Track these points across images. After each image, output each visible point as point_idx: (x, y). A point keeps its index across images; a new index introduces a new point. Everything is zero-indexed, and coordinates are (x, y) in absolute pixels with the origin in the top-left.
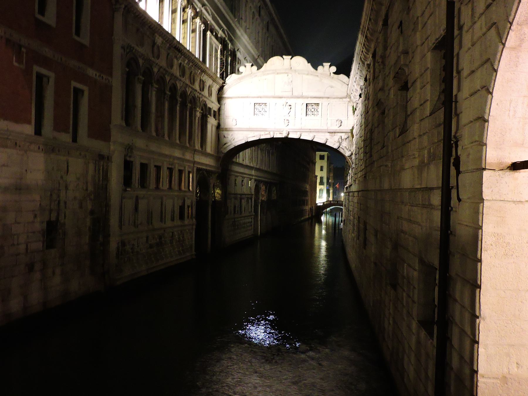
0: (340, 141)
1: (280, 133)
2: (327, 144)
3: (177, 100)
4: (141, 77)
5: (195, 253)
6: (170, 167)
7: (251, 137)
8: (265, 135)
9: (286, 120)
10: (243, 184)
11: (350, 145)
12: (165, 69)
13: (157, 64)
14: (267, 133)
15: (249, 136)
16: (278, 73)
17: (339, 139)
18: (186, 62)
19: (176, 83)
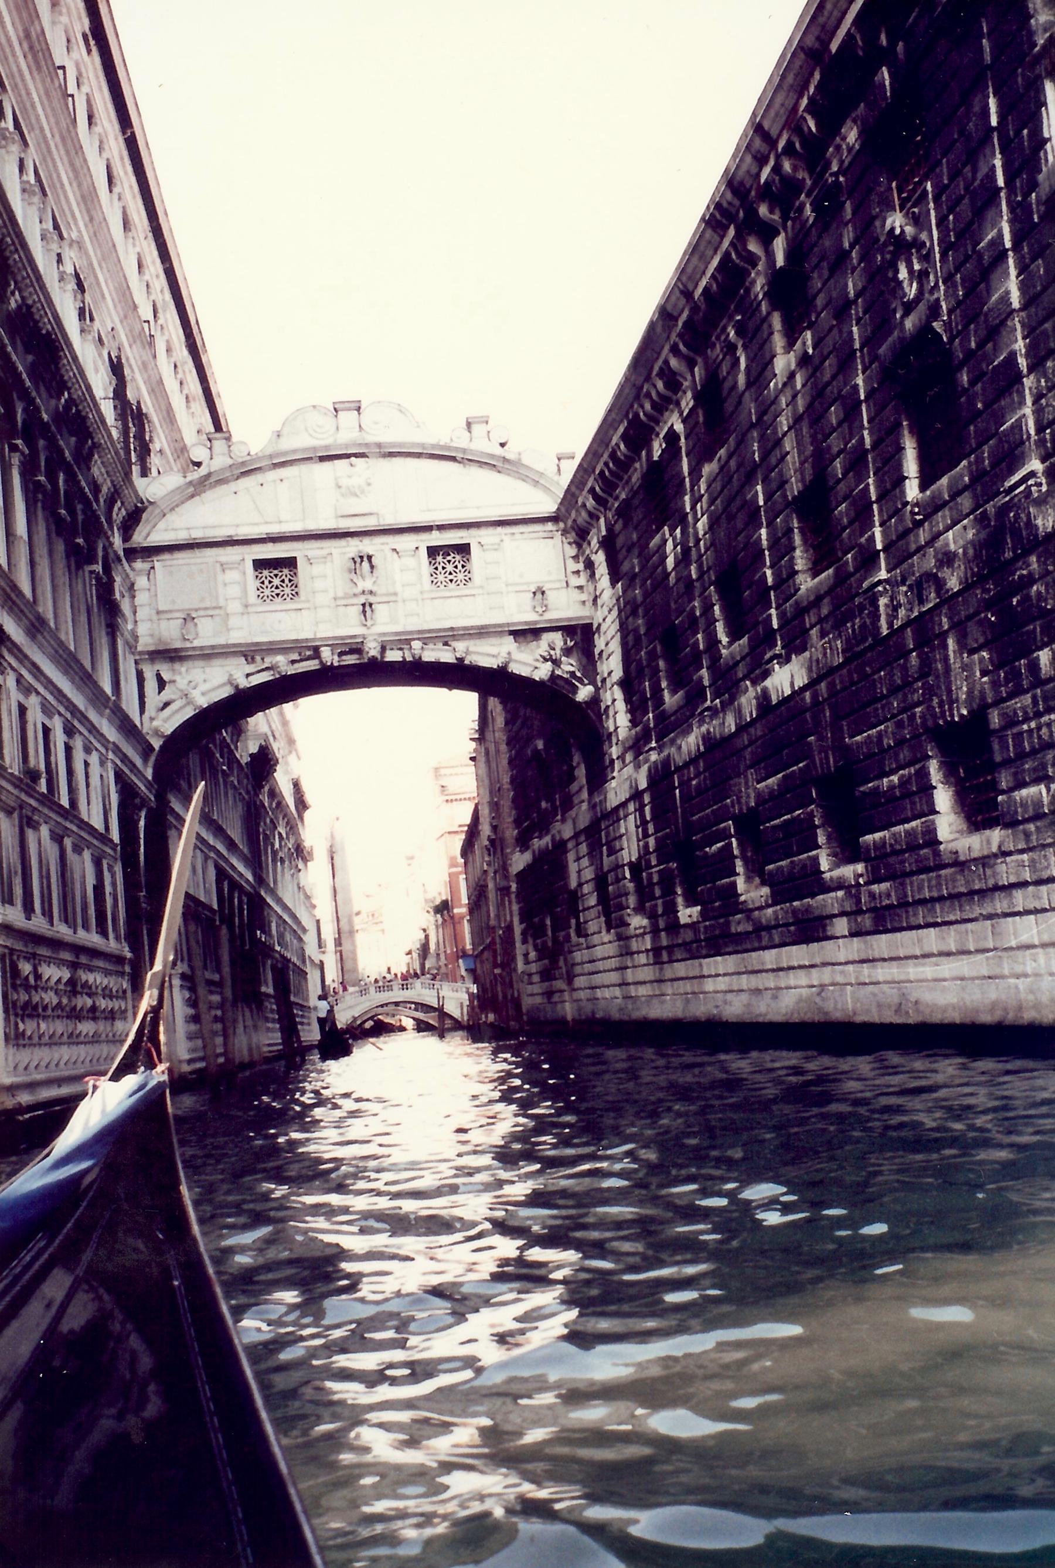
8: (301, 660)
15: (251, 668)
16: (322, 459)
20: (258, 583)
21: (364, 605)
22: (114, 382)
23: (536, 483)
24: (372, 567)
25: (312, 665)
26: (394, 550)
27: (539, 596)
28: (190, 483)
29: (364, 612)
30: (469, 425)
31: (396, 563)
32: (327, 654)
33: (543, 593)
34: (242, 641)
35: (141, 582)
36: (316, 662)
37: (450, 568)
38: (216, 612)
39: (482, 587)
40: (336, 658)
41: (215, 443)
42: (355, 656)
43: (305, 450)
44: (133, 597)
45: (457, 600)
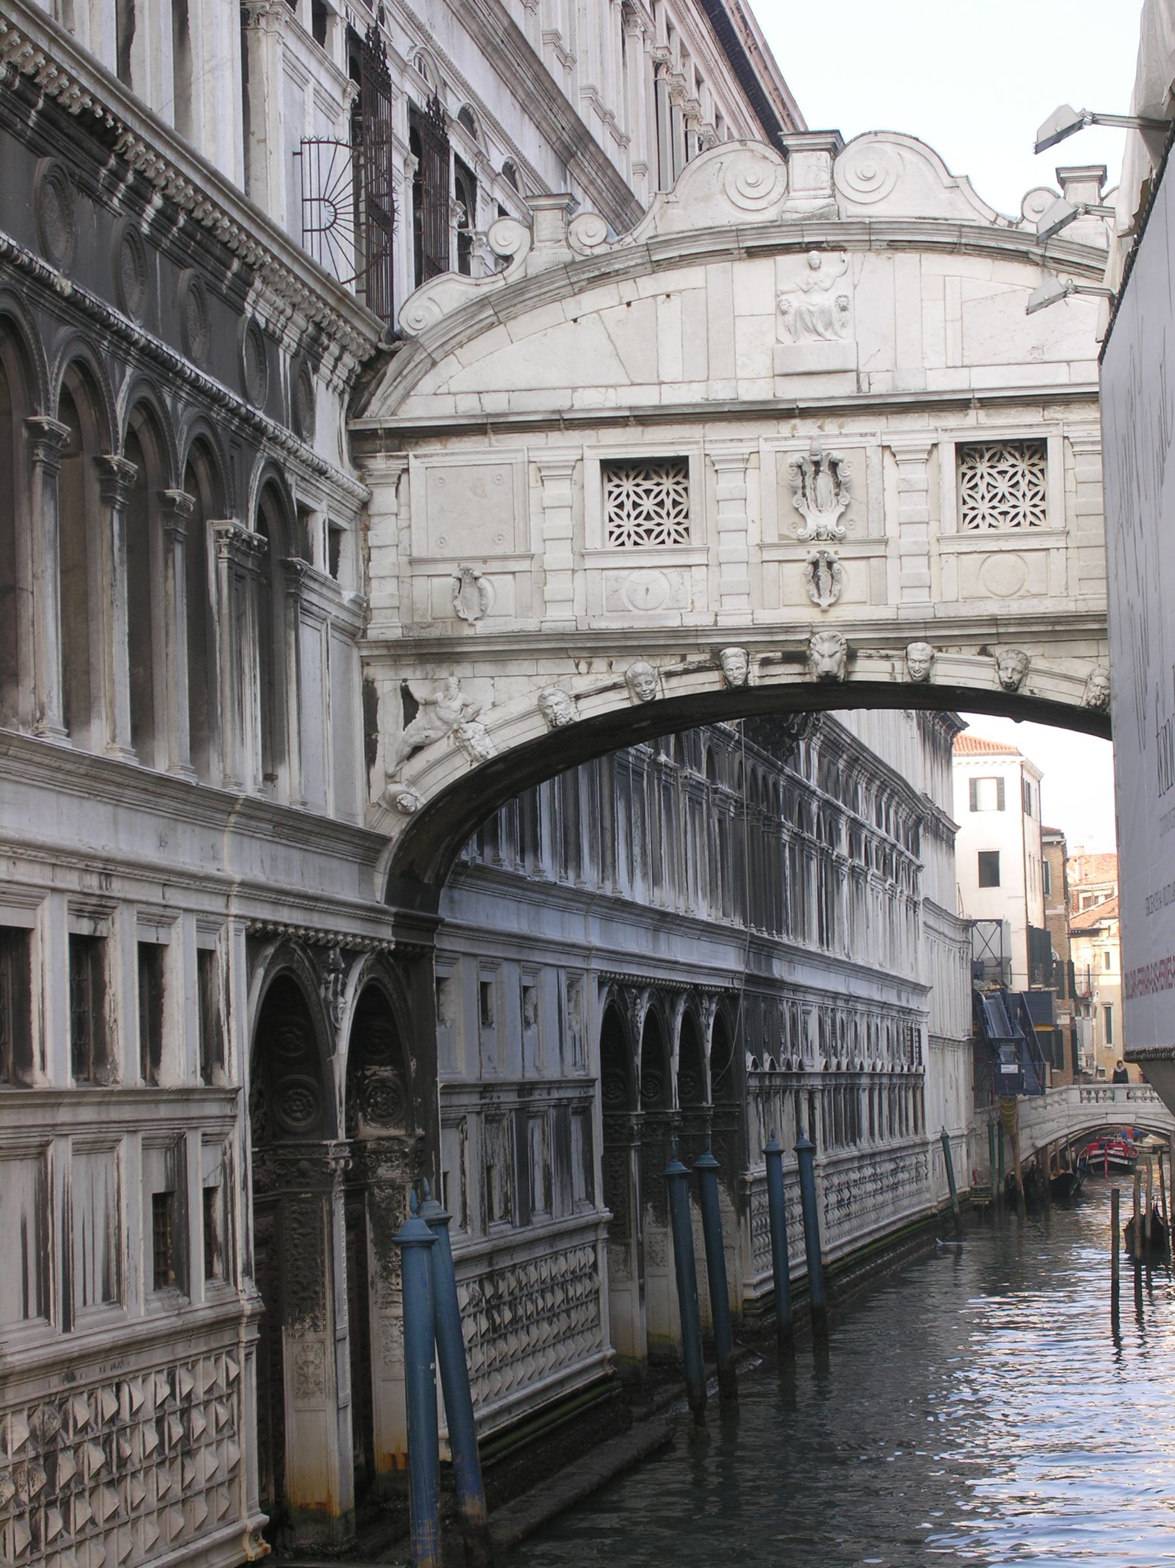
1: (790, 658)
5: (265, 1518)
6: (85, 928)
7: (587, 695)
8: (686, 672)
9: (822, 564)
10: (530, 1013)
12: (26, 270)
15: (582, 684)
16: (753, 253)
18: (150, 212)
20: (610, 507)
21: (815, 564)
22: (353, 90)
24: (838, 484)
25: (708, 682)
26: (884, 447)
28: (483, 302)
29: (816, 578)
30: (1062, 182)
32: (734, 659)
34: (569, 627)
35: (384, 498)
36: (715, 676)
37: (1003, 486)
38: (524, 565)
40: (755, 670)
42: (796, 668)
44: (367, 528)
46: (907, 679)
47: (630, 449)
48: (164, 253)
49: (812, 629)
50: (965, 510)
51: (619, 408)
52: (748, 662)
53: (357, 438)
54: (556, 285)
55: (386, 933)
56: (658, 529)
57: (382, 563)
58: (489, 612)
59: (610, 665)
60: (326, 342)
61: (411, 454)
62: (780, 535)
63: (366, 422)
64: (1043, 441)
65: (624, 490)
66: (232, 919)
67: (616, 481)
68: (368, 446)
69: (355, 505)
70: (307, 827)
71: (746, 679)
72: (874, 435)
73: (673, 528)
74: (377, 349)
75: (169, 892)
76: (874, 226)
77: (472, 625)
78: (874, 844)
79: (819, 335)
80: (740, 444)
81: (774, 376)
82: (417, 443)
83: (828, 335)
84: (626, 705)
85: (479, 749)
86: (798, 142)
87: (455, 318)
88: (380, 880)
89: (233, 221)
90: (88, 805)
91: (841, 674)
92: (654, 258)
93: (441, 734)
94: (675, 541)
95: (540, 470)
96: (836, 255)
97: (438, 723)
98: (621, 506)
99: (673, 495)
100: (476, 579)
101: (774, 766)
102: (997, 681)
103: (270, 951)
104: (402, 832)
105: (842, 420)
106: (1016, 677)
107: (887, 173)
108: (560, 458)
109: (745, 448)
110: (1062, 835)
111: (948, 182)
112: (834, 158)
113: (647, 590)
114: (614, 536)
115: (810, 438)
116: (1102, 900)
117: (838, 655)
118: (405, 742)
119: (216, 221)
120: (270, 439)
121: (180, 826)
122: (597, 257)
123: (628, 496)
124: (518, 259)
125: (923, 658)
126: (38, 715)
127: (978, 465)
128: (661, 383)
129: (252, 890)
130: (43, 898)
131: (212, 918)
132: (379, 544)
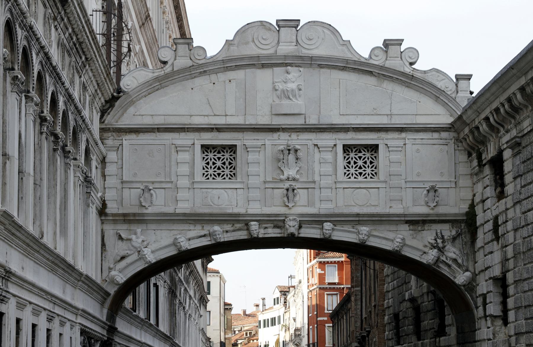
0: (441, 245)
1: (276, 227)
2: (403, 253)
3: (56, 136)
4: (21, 75)
7: (193, 238)
8: (234, 231)
9: (290, 190)
11: (467, 253)
13: (38, 39)
14: (238, 226)
15: (192, 234)
16: (264, 66)
17: (435, 240)
18: (67, 35)
19: (57, 94)
21: (287, 190)
23: (437, 99)
24: (297, 159)
25: (242, 235)
26: (316, 145)
27: (432, 193)
28: (157, 79)
31: (317, 155)
32: (254, 226)
33: (436, 191)
34: (188, 211)
35: (112, 156)
36: (245, 232)
37: (360, 163)
38: (169, 185)
39: (386, 182)
40: (262, 231)
41: (179, 46)
42: (278, 230)
43: (251, 58)
45: (364, 190)
46: (322, 237)
47: (213, 141)
48: (68, 51)
49: (286, 216)
50: (345, 171)
51: (211, 124)
52: (259, 228)
53: (102, 130)
54: (185, 74)
55: (105, 333)
56: (222, 173)
57: (111, 181)
58: (154, 203)
59: (203, 227)
60: (98, 91)
61: (124, 139)
62: (273, 178)
63: (106, 125)
64: (377, 146)
65: (209, 157)
66: (78, 324)
67: (206, 153)
68: (106, 135)
69: (101, 157)
70: (94, 288)
71: (258, 236)
72: (311, 140)
73: (229, 173)
74: (112, 95)
75: (66, 311)
76: (313, 58)
77: (147, 209)
78: (193, 306)
79: (290, 99)
80: (258, 141)
81: (272, 115)
82: (126, 134)
83: (294, 100)
84: (209, 243)
85: (149, 259)
86: (284, 23)
87: (144, 85)
88: (105, 311)
89: (89, 40)
90: (50, 274)
91: (296, 234)
92: (225, 66)
93: (132, 252)
94: (230, 179)
95: (176, 147)
96: (297, 68)
97: (132, 248)
98: (208, 163)
99: (229, 160)
100: (150, 190)
101: (176, 273)
102: (358, 239)
103: (83, 338)
104: (115, 291)
105: (298, 133)
106: (366, 237)
107: (318, 38)
108: (185, 143)
109: (260, 143)
110: (231, 305)
111: (341, 42)
112: (297, 31)
113: (219, 197)
114: (205, 175)
115: (285, 140)
116: (237, 332)
117: (296, 226)
118: (118, 255)
119: (84, 39)
120: (88, 129)
121: (67, 285)
122: (202, 64)
123: (211, 159)
124: (170, 63)
125: (330, 229)
126: (41, 236)
127: (351, 154)
128: (226, 115)
129: (85, 314)
130: (41, 312)
131: (73, 324)
132: (109, 174)
